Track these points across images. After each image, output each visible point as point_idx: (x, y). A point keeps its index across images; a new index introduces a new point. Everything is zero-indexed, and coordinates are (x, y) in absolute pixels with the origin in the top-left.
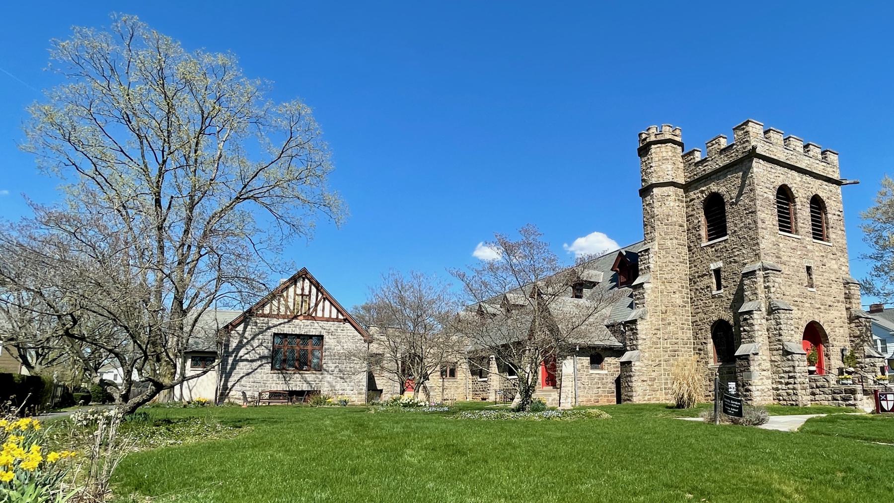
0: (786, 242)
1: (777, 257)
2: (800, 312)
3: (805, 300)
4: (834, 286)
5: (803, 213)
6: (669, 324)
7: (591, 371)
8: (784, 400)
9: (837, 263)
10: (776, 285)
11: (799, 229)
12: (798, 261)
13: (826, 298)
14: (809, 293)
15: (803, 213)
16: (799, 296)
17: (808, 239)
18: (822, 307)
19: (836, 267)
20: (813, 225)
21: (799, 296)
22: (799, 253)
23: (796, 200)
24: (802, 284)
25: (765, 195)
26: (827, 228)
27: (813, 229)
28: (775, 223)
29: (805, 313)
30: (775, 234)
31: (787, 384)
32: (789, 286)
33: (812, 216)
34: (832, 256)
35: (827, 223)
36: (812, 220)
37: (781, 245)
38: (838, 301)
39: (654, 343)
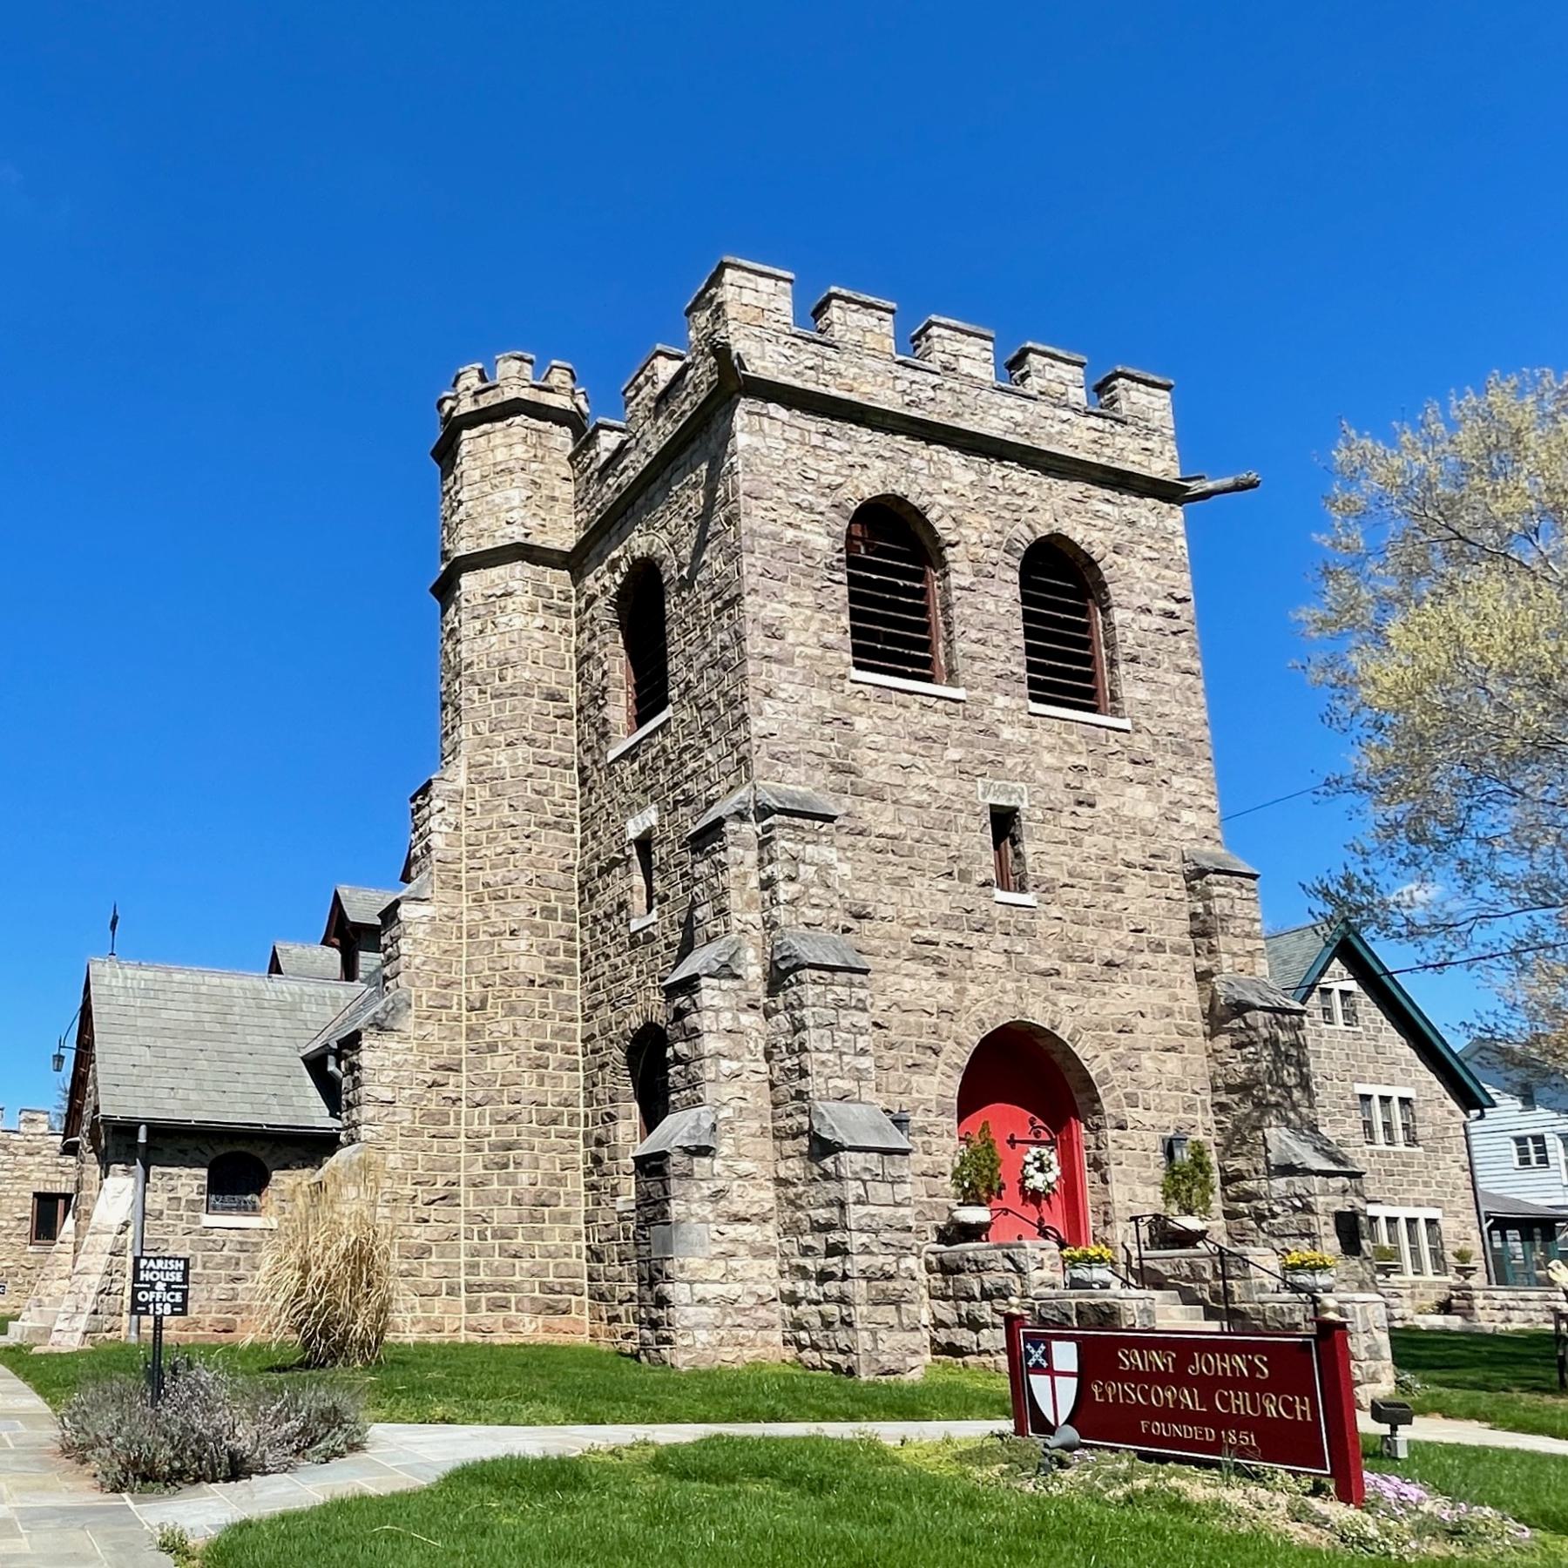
0: (890, 711)
1: (836, 769)
2: (948, 987)
3: (974, 940)
4: (1136, 885)
5: (983, 610)
6: (492, 1048)
7: (208, 1220)
8: (815, 1347)
9: (1154, 798)
10: (807, 872)
11: (960, 663)
12: (949, 786)
13: (1090, 933)
14: (998, 913)
15: (983, 610)
16: (945, 922)
17: (1001, 701)
18: (1070, 968)
19: (1148, 811)
20: (1030, 650)
21: (945, 922)
22: (954, 754)
23: (949, 553)
24: (964, 876)
25: (790, 534)
26: (1113, 663)
27: (1031, 667)
28: (830, 638)
29: (973, 990)
30: (830, 682)
31: (824, 1277)
32: (895, 882)
33: (1027, 616)
34: (1128, 770)
35: (1110, 645)
36: (1028, 633)
37: (861, 724)
38: (1159, 947)
39: (428, 1116)
